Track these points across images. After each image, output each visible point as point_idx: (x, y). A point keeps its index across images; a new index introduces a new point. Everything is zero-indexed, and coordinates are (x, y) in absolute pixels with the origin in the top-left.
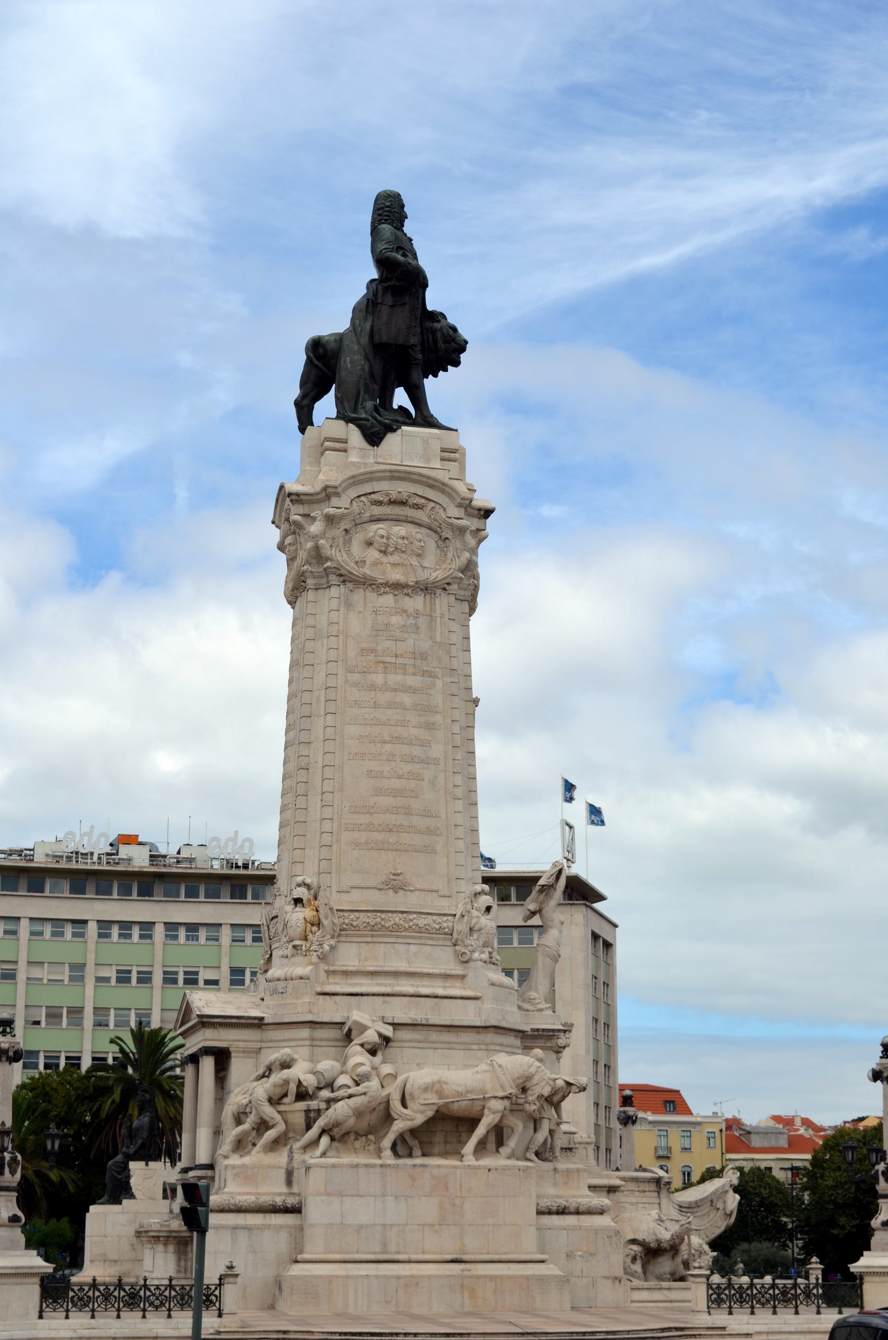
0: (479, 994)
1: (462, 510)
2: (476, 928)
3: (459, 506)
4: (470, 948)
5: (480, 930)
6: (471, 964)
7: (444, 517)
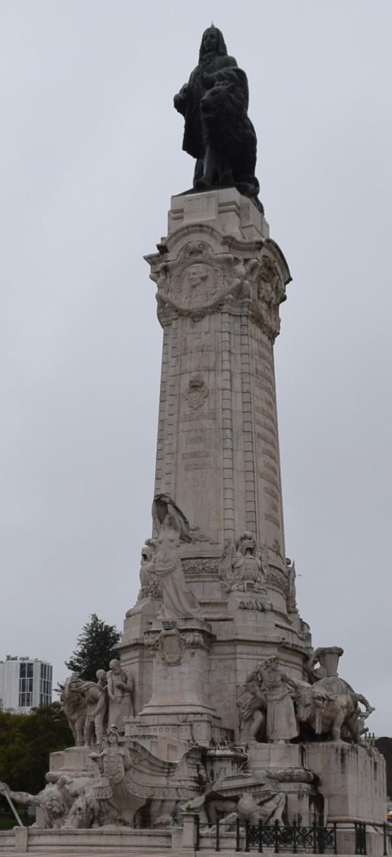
0: (230, 617)
1: (227, 247)
2: (236, 566)
3: (224, 243)
4: (230, 582)
5: (238, 568)
6: (232, 594)
7: (211, 254)
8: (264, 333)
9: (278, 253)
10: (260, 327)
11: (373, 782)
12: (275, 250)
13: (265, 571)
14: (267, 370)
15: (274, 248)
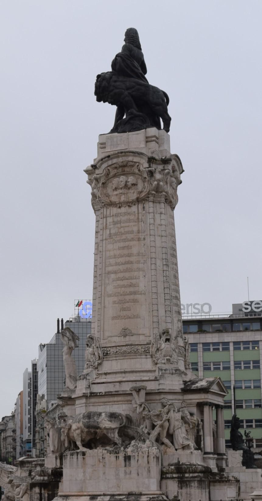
8: (120, 207)
9: (129, 154)
10: (116, 207)
11: (122, 470)
12: (123, 154)
13: (96, 354)
14: (122, 229)
15: (119, 154)
